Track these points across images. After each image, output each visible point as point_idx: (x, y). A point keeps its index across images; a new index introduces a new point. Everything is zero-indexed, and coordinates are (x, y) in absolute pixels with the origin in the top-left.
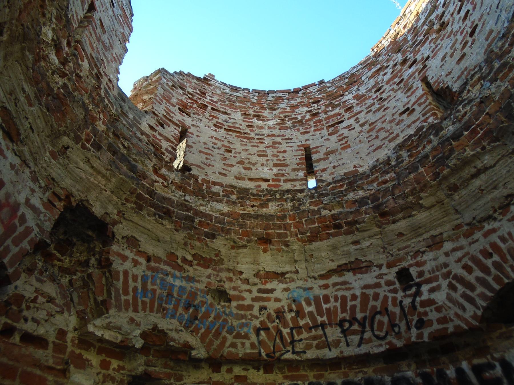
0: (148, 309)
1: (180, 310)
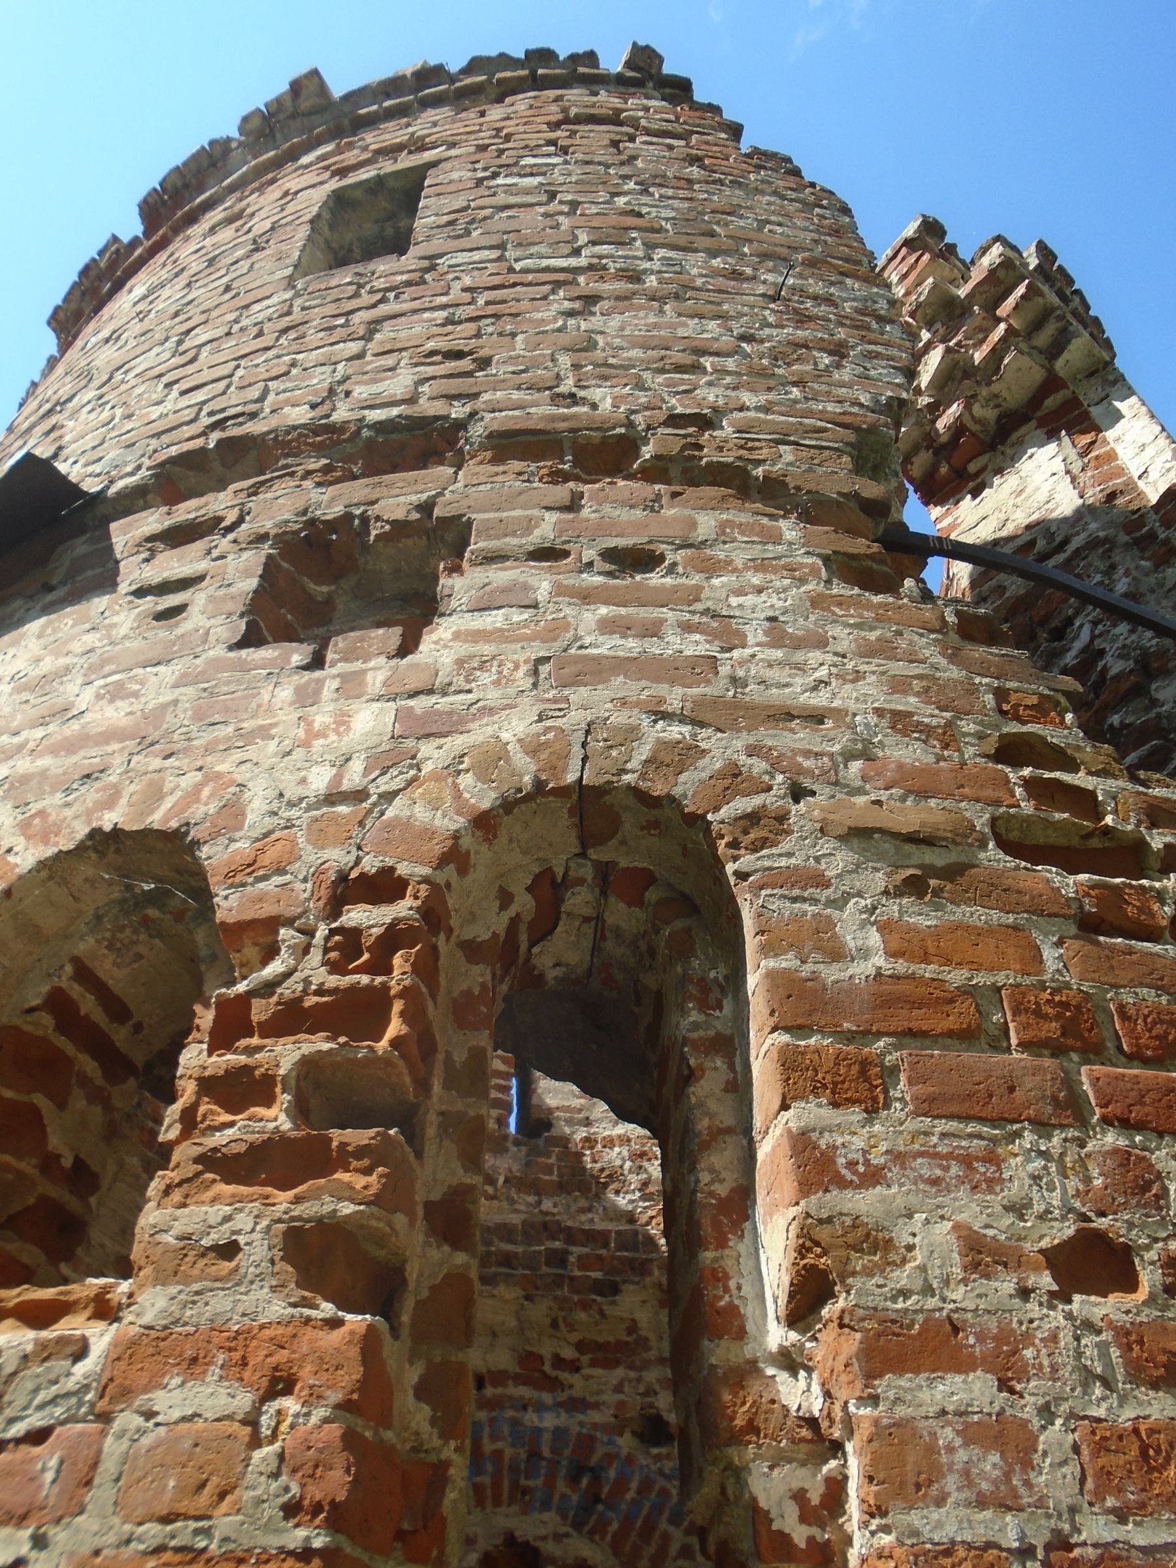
0: (489, 1502)
1: (561, 1487)
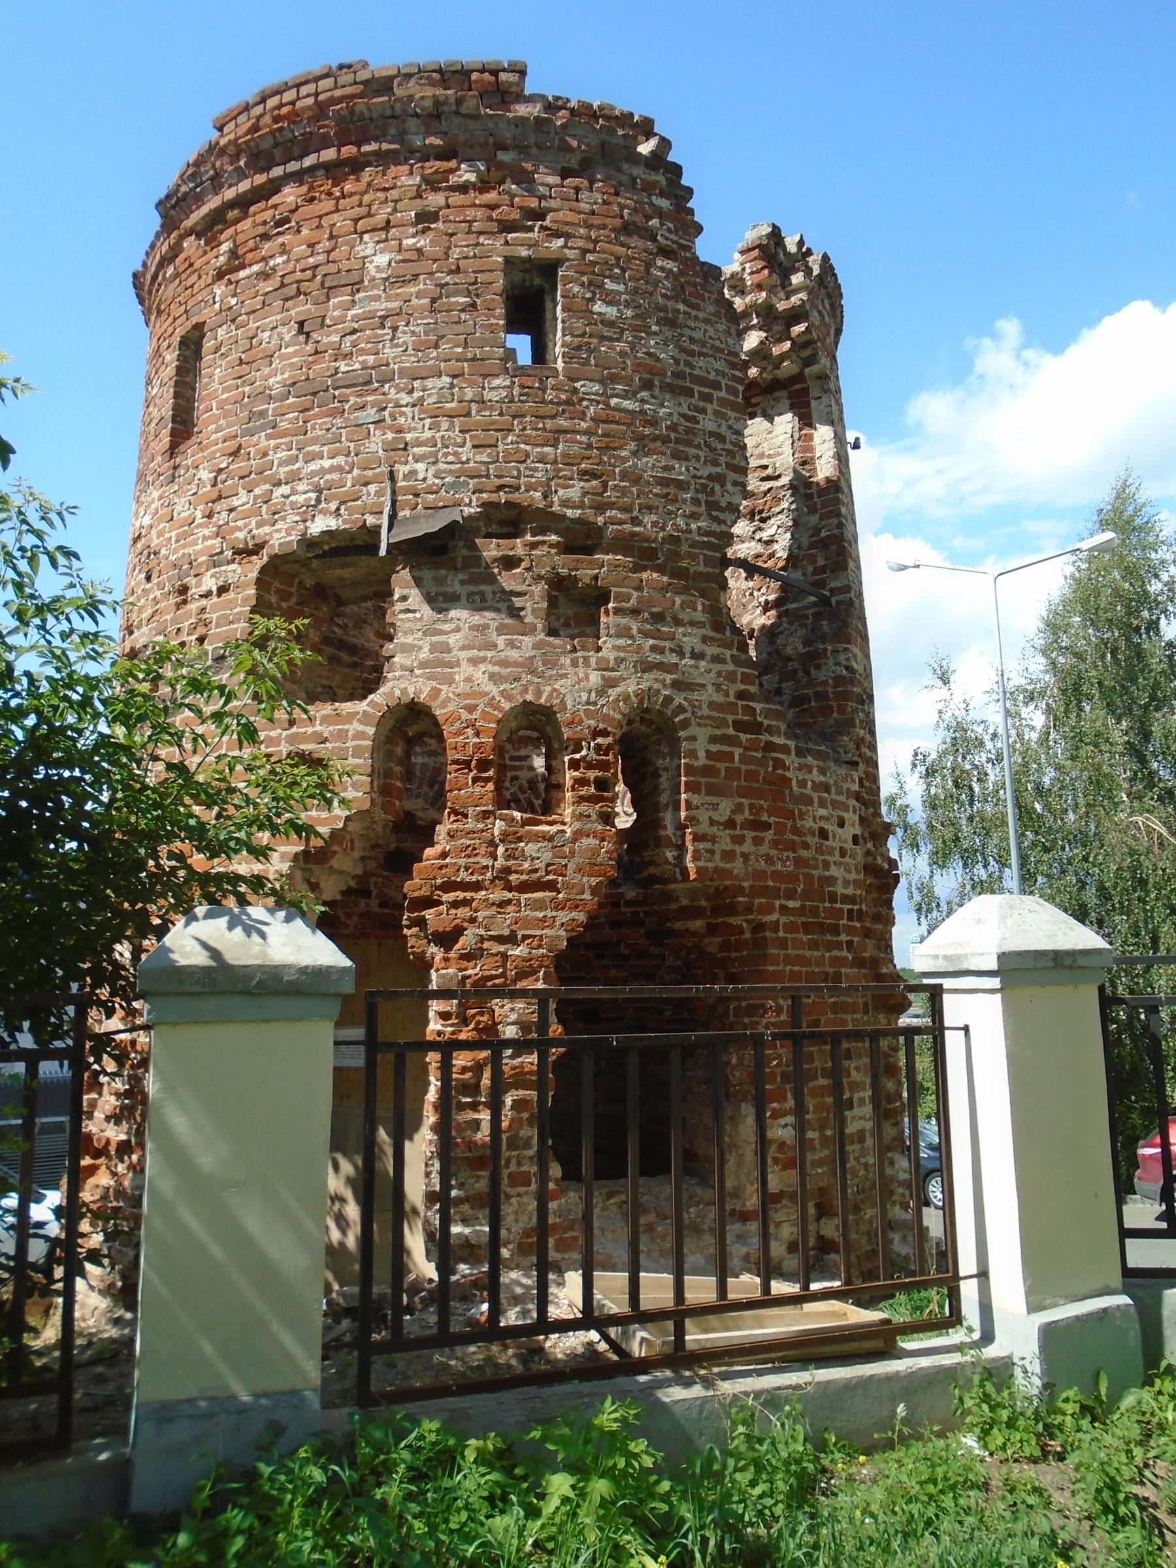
1: (425, 789)
